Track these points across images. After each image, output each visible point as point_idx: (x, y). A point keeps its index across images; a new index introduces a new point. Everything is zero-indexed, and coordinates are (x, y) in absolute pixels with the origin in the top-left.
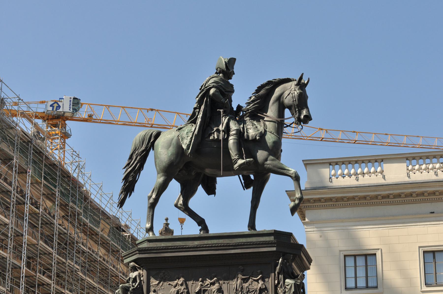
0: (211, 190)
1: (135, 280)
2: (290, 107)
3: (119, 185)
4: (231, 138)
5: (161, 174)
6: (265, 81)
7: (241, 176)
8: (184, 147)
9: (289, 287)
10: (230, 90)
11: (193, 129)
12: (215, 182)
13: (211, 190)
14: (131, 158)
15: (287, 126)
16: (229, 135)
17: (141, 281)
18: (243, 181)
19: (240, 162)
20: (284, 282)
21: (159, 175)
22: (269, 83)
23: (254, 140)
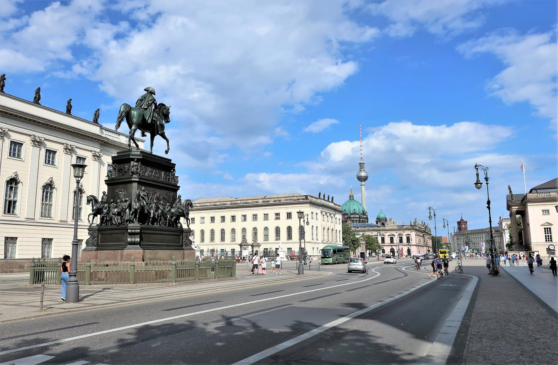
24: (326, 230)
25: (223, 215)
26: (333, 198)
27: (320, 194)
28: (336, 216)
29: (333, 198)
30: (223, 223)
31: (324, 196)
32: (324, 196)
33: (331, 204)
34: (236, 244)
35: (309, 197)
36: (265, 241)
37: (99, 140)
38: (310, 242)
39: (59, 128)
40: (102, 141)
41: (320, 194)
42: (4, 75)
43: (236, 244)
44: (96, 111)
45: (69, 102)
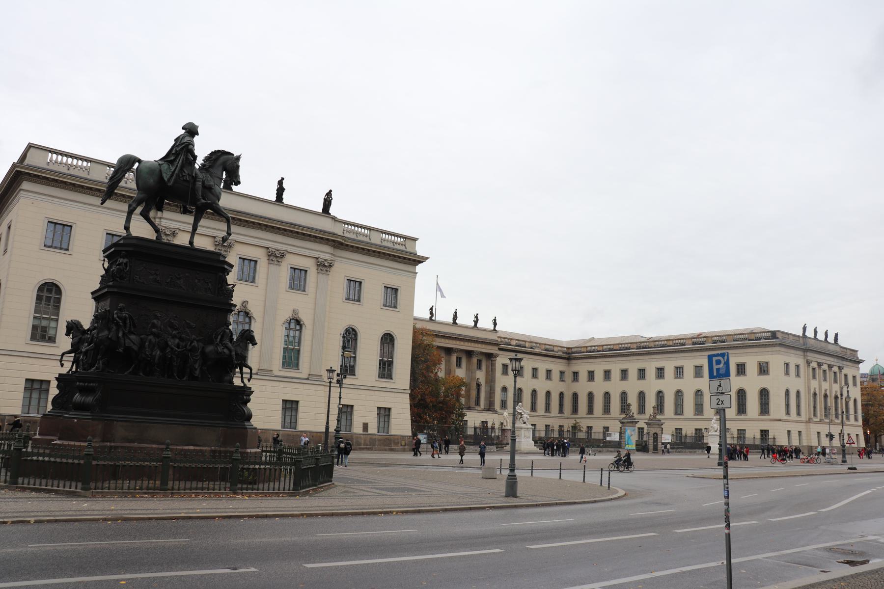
1: (126, 264)
11: (173, 169)
19: (203, 201)
22: (219, 151)
24: (820, 399)
25: (624, 367)
26: (836, 335)
27: (805, 329)
28: (844, 371)
29: (836, 335)
30: (624, 382)
31: (816, 332)
32: (816, 332)
33: (832, 348)
34: (615, 419)
35: (779, 335)
36: (695, 415)
37: (328, 239)
38: (780, 420)
39: (260, 224)
40: (334, 241)
41: (805, 329)
43: (615, 419)
44: (327, 194)
45: (280, 183)
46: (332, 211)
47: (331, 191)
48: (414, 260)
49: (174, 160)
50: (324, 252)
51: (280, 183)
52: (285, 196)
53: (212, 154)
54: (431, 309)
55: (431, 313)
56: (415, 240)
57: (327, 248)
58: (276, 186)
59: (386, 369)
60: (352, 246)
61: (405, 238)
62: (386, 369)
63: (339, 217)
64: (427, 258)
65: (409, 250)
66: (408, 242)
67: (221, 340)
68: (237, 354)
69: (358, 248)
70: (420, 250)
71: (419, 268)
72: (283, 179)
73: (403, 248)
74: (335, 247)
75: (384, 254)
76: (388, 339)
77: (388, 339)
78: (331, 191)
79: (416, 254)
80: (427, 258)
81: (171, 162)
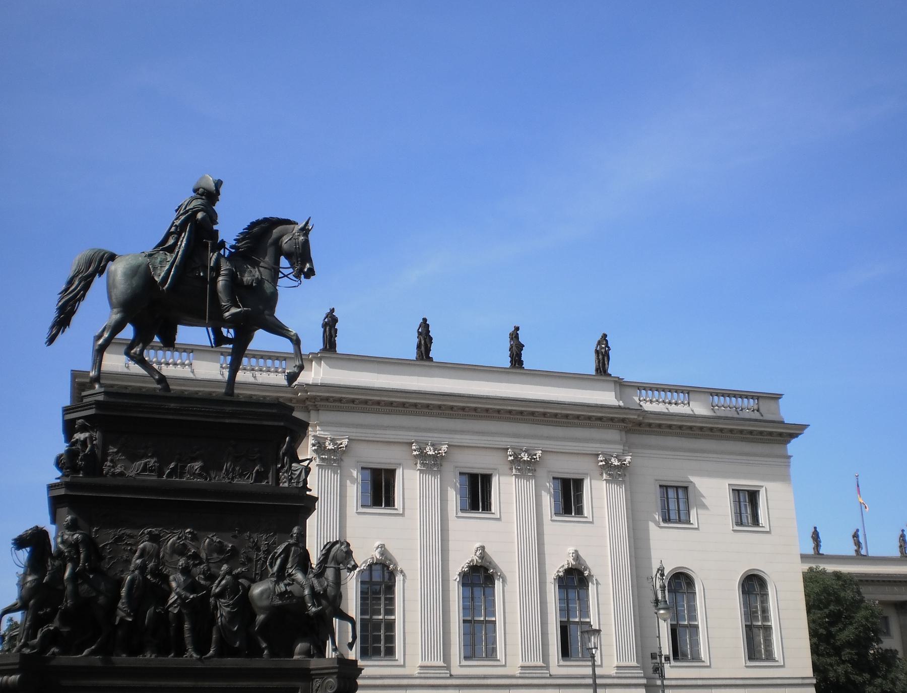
0: (169, 342)
2: (289, 256)
3: (51, 315)
4: (220, 278)
5: (119, 309)
6: (261, 217)
7: (210, 329)
8: (158, 279)
9: (298, 473)
10: (212, 217)
11: (170, 258)
12: (174, 331)
13: (169, 342)
14: (70, 282)
15: (285, 276)
16: (218, 275)
17: (93, 446)
18: (212, 337)
20: (290, 466)
21: (115, 310)
22: (266, 220)
23: (250, 287)
40: (623, 420)
42: (333, 310)
45: (515, 336)
46: (613, 369)
47: (605, 336)
48: (781, 434)
49: (175, 244)
50: (609, 442)
51: (515, 336)
52: (526, 356)
53: (253, 225)
54: (856, 535)
55: (858, 544)
56: (776, 397)
57: (614, 434)
58: (507, 344)
59: (757, 641)
60: (660, 426)
61: (757, 396)
62: (757, 641)
63: (628, 378)
64: (805, 427)
65: (768, 417)
66: (765, 406)
67: (283, 567)
68: (314, 594)
69: (670, 426)
70: (789, 413)
71: (793, 447)
72: (517, 329)
73: (756, 415)
74: (628, 431)
75: (721, 430)
76: (753, 585)
77: (753, 585)
78: (605, 336)
79: (783, 422)
80: (805, 427)
81: (171, 249)
